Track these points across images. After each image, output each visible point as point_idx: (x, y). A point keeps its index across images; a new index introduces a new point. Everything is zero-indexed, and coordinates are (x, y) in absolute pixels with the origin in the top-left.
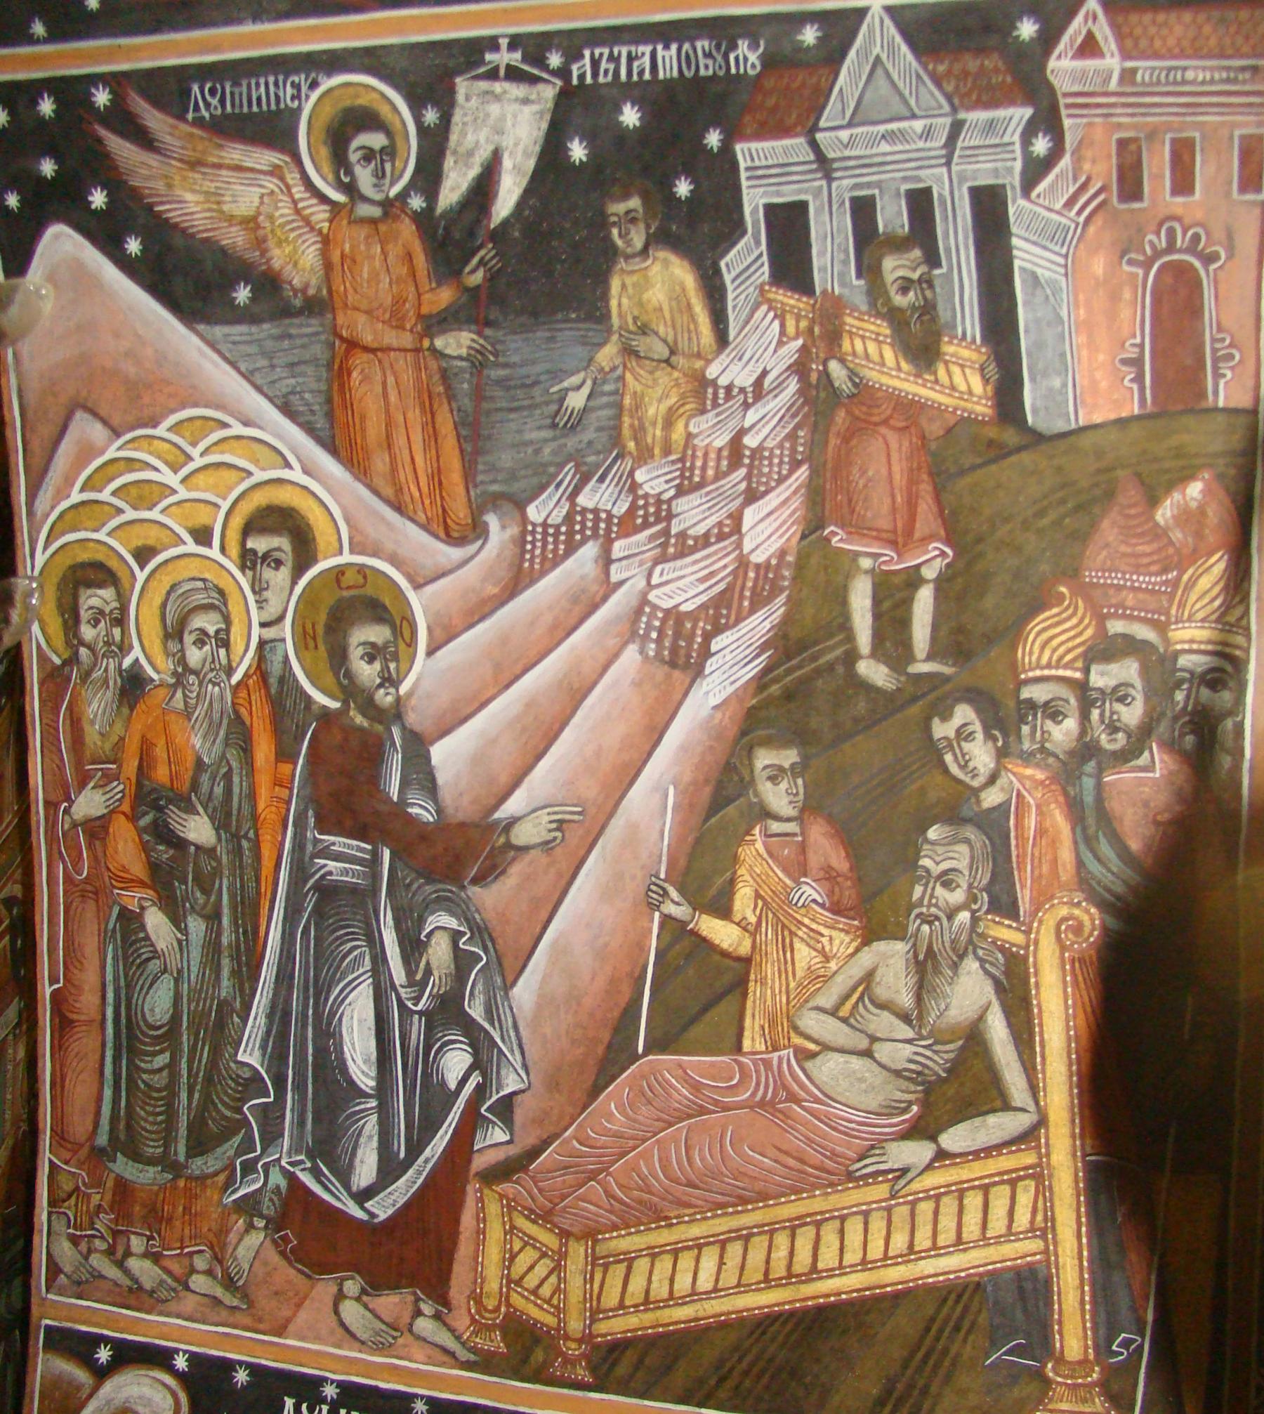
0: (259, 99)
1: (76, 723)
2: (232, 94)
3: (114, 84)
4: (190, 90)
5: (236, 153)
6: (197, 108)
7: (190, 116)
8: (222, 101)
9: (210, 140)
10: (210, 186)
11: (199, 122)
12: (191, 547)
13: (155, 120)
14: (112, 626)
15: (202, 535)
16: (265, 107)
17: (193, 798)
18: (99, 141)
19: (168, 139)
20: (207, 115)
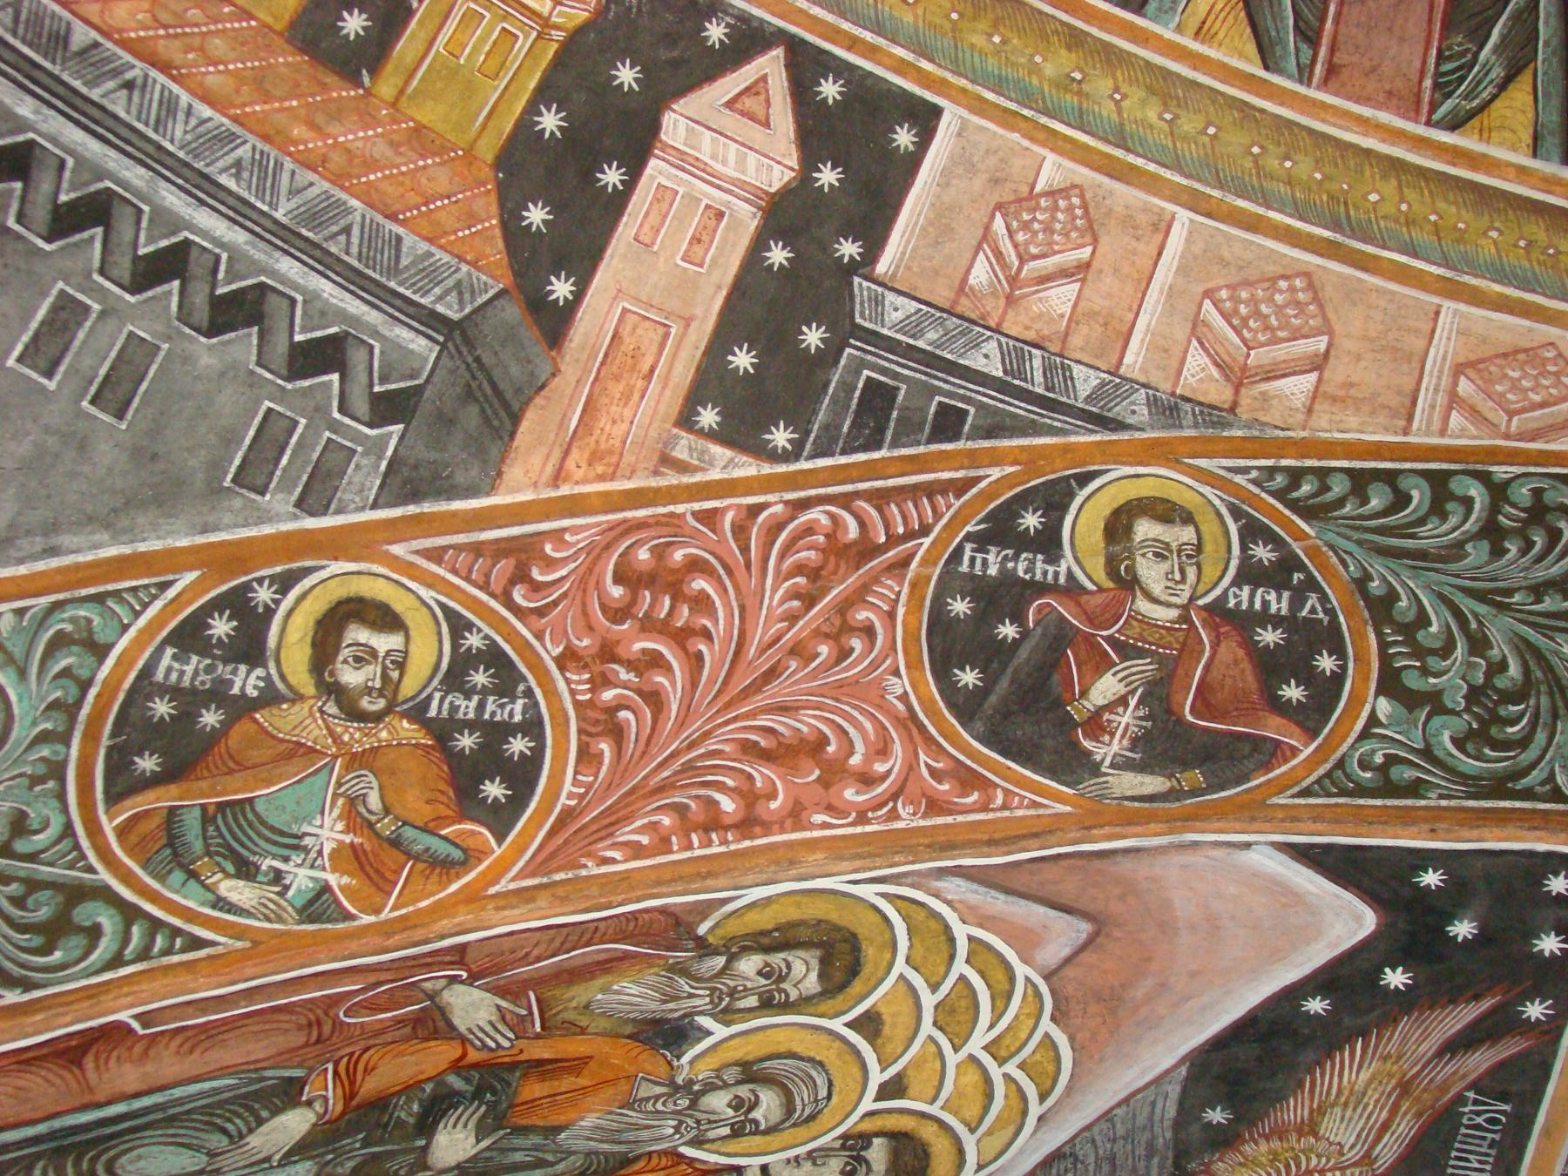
0: (1467, 1160)
1: (607, 966)
2: (1483, 1138)
3: (1546, 1027)
4: (1505, 1102)
5: (1405, 1127)
6: (1476, 1102)
7: (1471, 1095)
8: (1478, 1127)
9: (1432, 1107)
10: (1372, 1097)
11: (1460, 1099)
12: (877, 1078)
13: (1480, 1061)
14: (760, 995)
15: (894, 1088)
16: (1452, 1162)
17: (501, 1133)
18: (1477, 997)
19: (1449, 1069)
20: (1466, 1110)
